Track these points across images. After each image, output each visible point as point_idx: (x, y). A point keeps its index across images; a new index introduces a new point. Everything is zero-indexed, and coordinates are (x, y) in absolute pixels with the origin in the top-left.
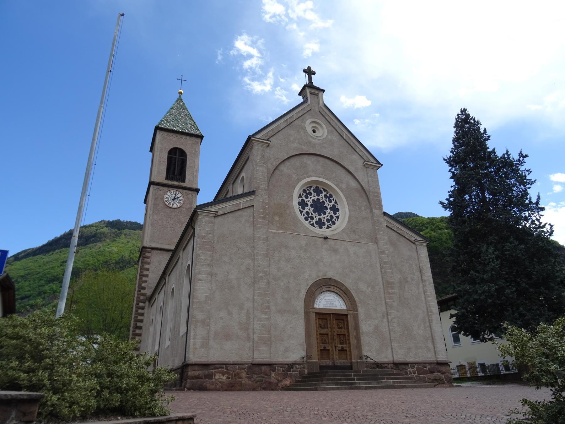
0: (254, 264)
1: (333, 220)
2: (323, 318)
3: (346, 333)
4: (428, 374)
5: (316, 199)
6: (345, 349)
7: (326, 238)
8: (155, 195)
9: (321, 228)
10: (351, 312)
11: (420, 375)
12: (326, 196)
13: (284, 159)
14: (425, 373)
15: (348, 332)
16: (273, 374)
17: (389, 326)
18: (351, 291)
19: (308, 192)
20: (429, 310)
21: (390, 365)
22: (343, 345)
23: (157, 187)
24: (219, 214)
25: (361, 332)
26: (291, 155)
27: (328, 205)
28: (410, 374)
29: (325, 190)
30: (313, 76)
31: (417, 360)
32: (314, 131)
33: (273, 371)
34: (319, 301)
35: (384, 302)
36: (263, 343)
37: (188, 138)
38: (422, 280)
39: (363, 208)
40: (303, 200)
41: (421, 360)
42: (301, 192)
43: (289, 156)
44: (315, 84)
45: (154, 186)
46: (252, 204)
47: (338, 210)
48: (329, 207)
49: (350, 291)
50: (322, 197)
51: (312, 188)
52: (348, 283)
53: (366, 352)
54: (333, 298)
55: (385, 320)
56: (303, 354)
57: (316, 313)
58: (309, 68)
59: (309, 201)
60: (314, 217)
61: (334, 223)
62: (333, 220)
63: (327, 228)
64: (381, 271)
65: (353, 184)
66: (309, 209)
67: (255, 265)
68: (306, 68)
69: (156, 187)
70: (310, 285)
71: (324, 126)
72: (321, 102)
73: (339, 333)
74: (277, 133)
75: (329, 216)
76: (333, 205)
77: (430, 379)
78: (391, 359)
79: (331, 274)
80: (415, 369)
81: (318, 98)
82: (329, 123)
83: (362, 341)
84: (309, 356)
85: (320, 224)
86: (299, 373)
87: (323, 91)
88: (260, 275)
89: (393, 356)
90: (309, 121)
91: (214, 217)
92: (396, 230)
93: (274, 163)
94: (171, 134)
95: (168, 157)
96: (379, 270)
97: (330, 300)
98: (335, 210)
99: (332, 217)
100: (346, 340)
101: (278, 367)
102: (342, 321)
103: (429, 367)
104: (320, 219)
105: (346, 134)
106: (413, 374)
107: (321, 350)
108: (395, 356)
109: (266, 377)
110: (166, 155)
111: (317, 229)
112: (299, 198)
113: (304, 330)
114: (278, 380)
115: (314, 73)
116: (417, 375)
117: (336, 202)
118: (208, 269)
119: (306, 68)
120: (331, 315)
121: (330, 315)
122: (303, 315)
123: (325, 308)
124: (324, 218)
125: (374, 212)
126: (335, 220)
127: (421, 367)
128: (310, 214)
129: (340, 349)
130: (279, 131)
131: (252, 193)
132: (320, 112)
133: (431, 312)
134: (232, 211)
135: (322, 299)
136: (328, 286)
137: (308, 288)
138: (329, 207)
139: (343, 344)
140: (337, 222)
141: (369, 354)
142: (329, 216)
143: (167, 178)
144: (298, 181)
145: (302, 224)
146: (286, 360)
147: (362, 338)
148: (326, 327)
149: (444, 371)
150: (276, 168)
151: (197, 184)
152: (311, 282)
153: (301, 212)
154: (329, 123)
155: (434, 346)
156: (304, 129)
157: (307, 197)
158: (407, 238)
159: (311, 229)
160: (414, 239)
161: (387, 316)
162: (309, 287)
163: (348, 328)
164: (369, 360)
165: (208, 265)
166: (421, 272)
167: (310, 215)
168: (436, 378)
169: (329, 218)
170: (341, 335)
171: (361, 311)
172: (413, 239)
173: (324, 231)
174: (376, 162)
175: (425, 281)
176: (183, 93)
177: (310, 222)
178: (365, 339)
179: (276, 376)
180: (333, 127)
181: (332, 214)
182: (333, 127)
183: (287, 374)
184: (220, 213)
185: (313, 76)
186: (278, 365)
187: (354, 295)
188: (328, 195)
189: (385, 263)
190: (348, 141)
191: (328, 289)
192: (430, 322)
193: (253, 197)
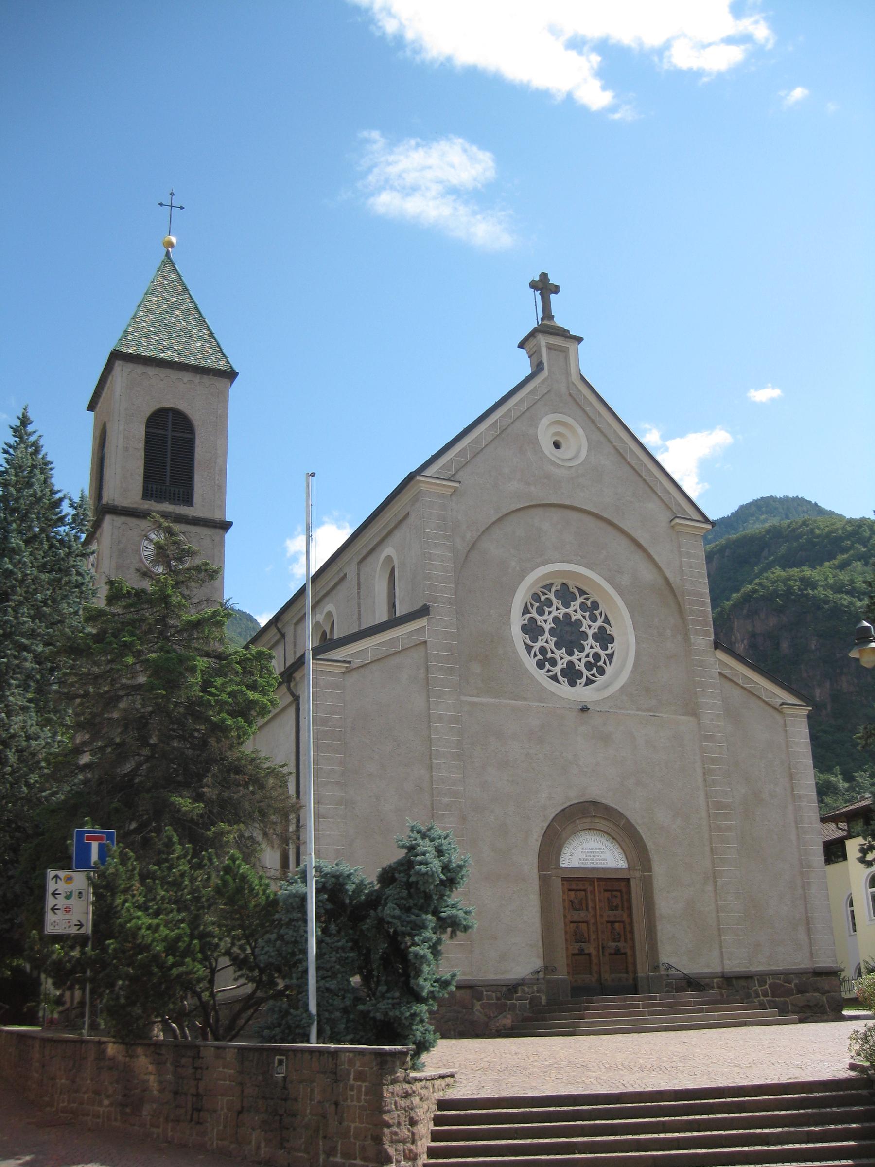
0: (432, 776)
1: (599, 664)
2: (578, 888)
3: (625, 918)
4: (793, 995)
5: (561, 616)
6: (623, 951)
7: (584, 709)
8: (119, 542)
9: (572, 684)
10: (637, 874)
12: (583, 607)
13: (491, 522)
15: (630, 915)
16: (478, 1006)
17: (716, 901)
18: (638, 827)
19: (543, 598)
20: (804, 863)
21: (715, 980)
23: (123, 519)
24: (354, 665)
25: (657, 914)
26: (505, 511)
27: (590, 627)
29: (582, 592)
30: (552, 296)
31: (774, 968)
32: (557, 445)
33: (479, 999)
34: (569, 853)
35: (708, 849)
36: (457, 945)
37: (197, 379)
38: (793, 795)
40: (532, 620)
41: (781, 968)
43: (500, 515)
44: (560, 321)
45: (116, 518)
46: (423, 639)
47: (611, 639)
48: (590, 633)
49: (636, 829)
50: (575, 611)
51: (553, 589)
53: (666, 956)
54: (600, 846)
55: (710, 888)
56: (537, 963)
57: (563, 879)
58: (544, 276)
59: (546, 621)
60: (558, 659)
61: (602, 672)
62: (601, 663)
63: (586, 684)
64: (705, 780)
65: (647, 574)
66: (547, 640)
67: (434, 778)
68: (537, 278)
69: (119, 520)
70: (551, 817)
71: (580, 431)
72: (573, 371)
73: (611, 919)
74: (474, 456)
75: (591, 655)
76: (601, 628)
78: (718, 969)
79: (598, 791)
80: (767, 986)
81: (567, 358)
82: (593, 422)
83: (659, 934)
84: (548, 968)
85: (571, 675)
86: (530, 1003)
87: (579, 340)
88: (446, 800)
89: (722, 961)
90: (545, 421)
92: (740, 682)
93: (468, 535)
94: (151, 371)
95: (147, 433)
96: (700, 779)
97: (592, 849)
98: (604, 638)
99: (597, 656)
100: (625, 932)
101: (487, 991)
102: (619, 894)
104: (571, 664)
106: (762, 998)
107: (573, 955)
108: (726, 962)
109: (464, 1011)
110: (140, 431)
111: (563, 689)
114: (489, 1017)
115: (556, 290)
116: (770, 998)
117: (607, 621)
119: (537, 278)
120: (596, 880)
121: (594, 881)
124: (580, 660)
125: (692, 641)
128: (549, 652)
129: (613, 951)
131: (424, 611)
132: (570, 395)
133: (809, 867)
134: (379, 657)
135: (576, 848)
136: (589, 820)
137: (546, 825)
138: (590, 633)
139: (619, 941)
140: (609, 669)
141: (672, 961)
142: (591, 655)
143: (147, 494)
144: (522, 575)
145: (532, 678)
146: (503, 977)
147: (659, 928)
148: (584, 906)
149: (827, 987)
150: (473, 546)
151: (222, 507)
152: (552, 813)
153: (529, 648)
154: (593, 422)
155: (810, 939)
156: (534, 442)
157: (541, 612)
158: (764, 701)
159: (552, 689)
160: (780, 701)
161: (715, 877)
163: (630, 908)
164: (672, 972)
165: (337, 783)
166: (791, 777)
167: (550, 655)
169: (591, 659)
170: (616, 922)
171: (660, 871)
173: (581, 693)
174: (701, 519)
176: (175, 244)
177: (549, 671)
178: (664, 930)
179: (483, 1009)
180: (602, 432)
181: (598, 649)
182: (602, 432)
183: (506, 1004)
184: (356, 662)
185: (552, 296)
186: (487, 988)
187: (644, 837)
188: (589, 603)
189: (714, 761)
190: (636, 467)
192: (803, 887)
193: (422, 622)
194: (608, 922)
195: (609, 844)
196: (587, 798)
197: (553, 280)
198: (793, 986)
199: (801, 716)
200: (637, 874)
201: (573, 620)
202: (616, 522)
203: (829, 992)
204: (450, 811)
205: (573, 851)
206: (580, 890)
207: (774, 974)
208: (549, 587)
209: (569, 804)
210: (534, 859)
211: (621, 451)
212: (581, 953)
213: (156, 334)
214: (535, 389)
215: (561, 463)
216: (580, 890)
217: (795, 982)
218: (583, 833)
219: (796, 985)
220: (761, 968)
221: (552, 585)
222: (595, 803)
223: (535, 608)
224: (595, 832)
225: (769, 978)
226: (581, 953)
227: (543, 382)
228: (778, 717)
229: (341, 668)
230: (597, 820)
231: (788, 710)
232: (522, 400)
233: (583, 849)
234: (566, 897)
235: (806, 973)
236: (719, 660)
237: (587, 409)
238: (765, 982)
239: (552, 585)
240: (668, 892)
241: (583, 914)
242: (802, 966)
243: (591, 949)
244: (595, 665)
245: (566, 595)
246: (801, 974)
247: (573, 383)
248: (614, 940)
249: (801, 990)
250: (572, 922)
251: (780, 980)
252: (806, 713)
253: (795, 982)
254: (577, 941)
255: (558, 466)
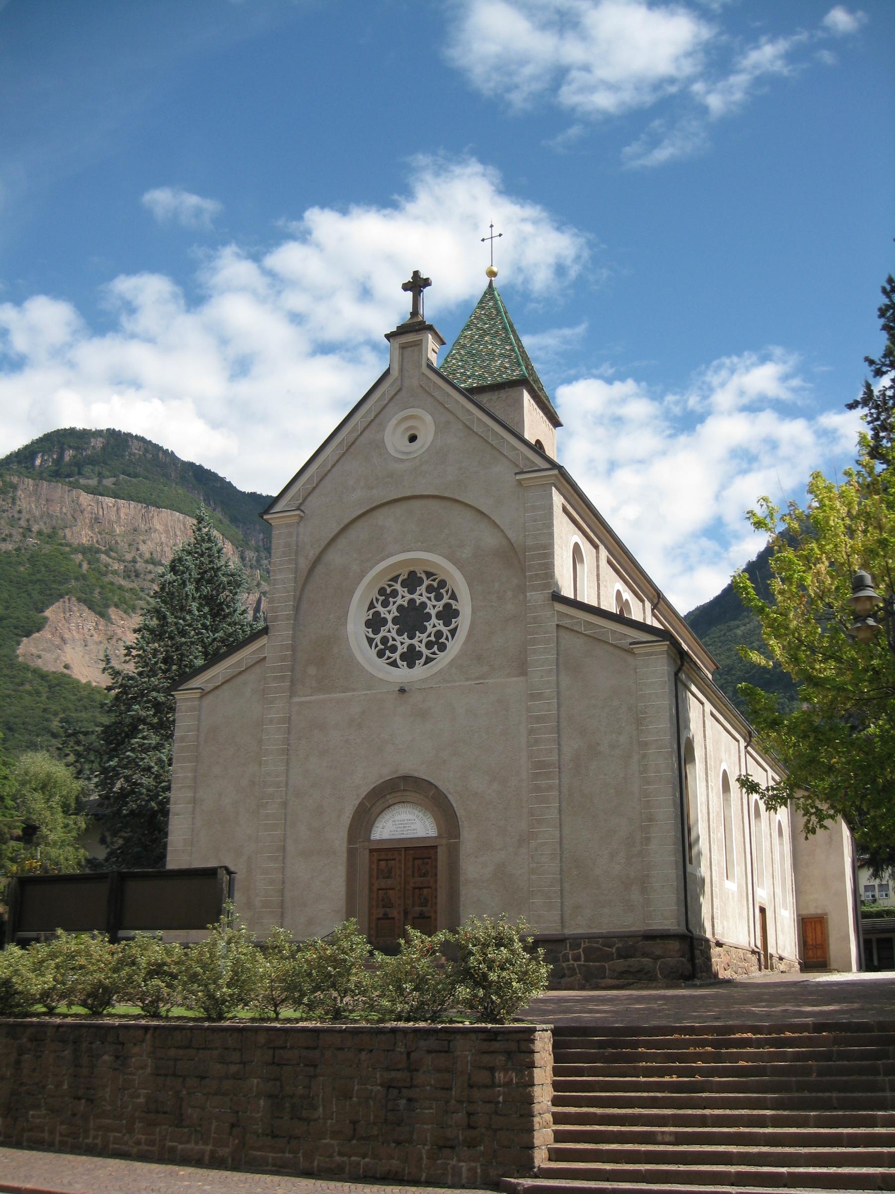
4: (613, 960)
7: (402, 691)
9: (411, 665)
10: (444, 841)
11: (591, 964)
14: (608, 957)
18: (449, 796)
22: (424, 909)
25: (462, 879)
26: (346, 521)
28: (563, 962)
29: (429, 574)
34: (381, 826)
39: (509, 594)
42: (374, 594)
43: (342, 526)
49: (447, 797)
52: (446, 782)
57: (371, 851)
59: (389, 612)
61: (442, 648)
71: (428, 418)
74: (321, 480)
77: (614, 971)
80: (581, 950)
81: (420, 350)
83: (462, 899)
88: (271, 790)
90: (394, 421)
91: (201, 697)
97: (403, 820)
102: (429, 861)
103: (620, 945)
105: (479, 419)
106: (572, 962)
112: (369, 609)
113: (344, 884)
116: (582, 963)
118: (190, 794)
120: (403, 850)
122: (343, 857)
123: (393, 837)
126: (389, 658)
127: (598, 946)
128: (391, 639)
130: (326, 475)
134: (227, 678)
136: (399, 794)
137: (357, 802)
149: (658, 952)
152: (364, 791)
156: (380, 446)
158: (612, 644)
162: (360, 800)
168: (630, 970)
171: (468, 837)
172: (625, 643)
173: (420, 671)
174: (547, 466)
175: (646, 744)
180: (451, 412)
182: (451, 412)
184: (210, 686)
187: (454, 805)
189: (539, 719)
191: (398, 800)
193: (264, 640)
194: (415, 888)
195: (421, 814)
196: (401, 773)
197: (424, 275)
198: (614, 950)
199: (661, 653)
200: (444, 841)
201: (406, 605)
202: (458, 498)
203: (663, 957)
204: (273, 799)
205: (385, 824)
206: (390, 860)
207: (591, 938)
208: (395, 579)
209: (383, 780)
210: (343, 834)
211: (468, 423)
212: (386, 917)
213: (462, 367)
214: (384, 394)
215: (404, 457)
216: (390, 860)
217: (617, 945)
218: (396, 807)
219: (617, 949)
220: (580, 931)
221: (398, 576)
222: (405, 778)
223: (380, 602)
224: (408, 805)
225: (584, 942)
226: (386, 917)
227: (392, 385)
228: (630, 659)
229: (196, 694)
230: (408, 793)
231: (638, 649)
232: (369, 411)
233: (394, 821)
234: (374, 866)
235: (635, 936)
236: (558, 612)
237: (436, 394)
238: (579, 946)
239: (398, 576)
240: (476, 857)
241: (390, 882)
242: (633, 929)
243: (394, 913)
244: (437, 642)
245: (412, 582)
246: (629, 937)
247: (423, 374)
248: (421, 905)
249: (624, 955)
250: (380, 889)
251: (597, 943)
252: (665, 648)
253: (617, 945)
254: (384, 907)
255: (402, 461)
